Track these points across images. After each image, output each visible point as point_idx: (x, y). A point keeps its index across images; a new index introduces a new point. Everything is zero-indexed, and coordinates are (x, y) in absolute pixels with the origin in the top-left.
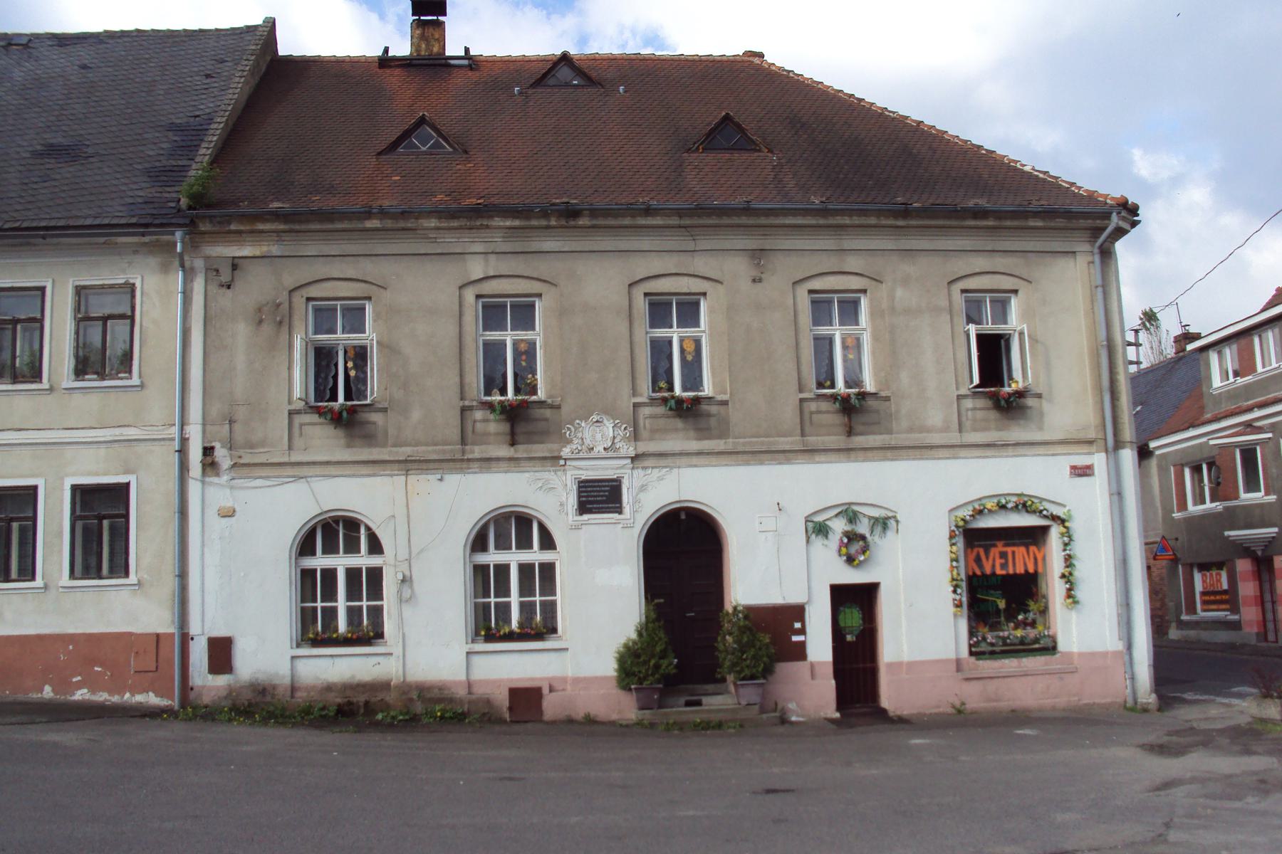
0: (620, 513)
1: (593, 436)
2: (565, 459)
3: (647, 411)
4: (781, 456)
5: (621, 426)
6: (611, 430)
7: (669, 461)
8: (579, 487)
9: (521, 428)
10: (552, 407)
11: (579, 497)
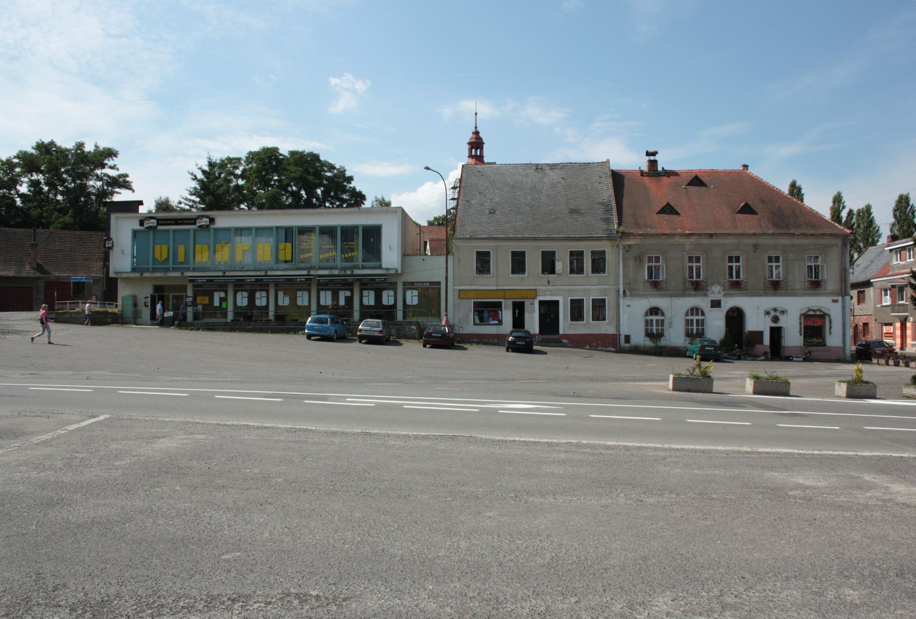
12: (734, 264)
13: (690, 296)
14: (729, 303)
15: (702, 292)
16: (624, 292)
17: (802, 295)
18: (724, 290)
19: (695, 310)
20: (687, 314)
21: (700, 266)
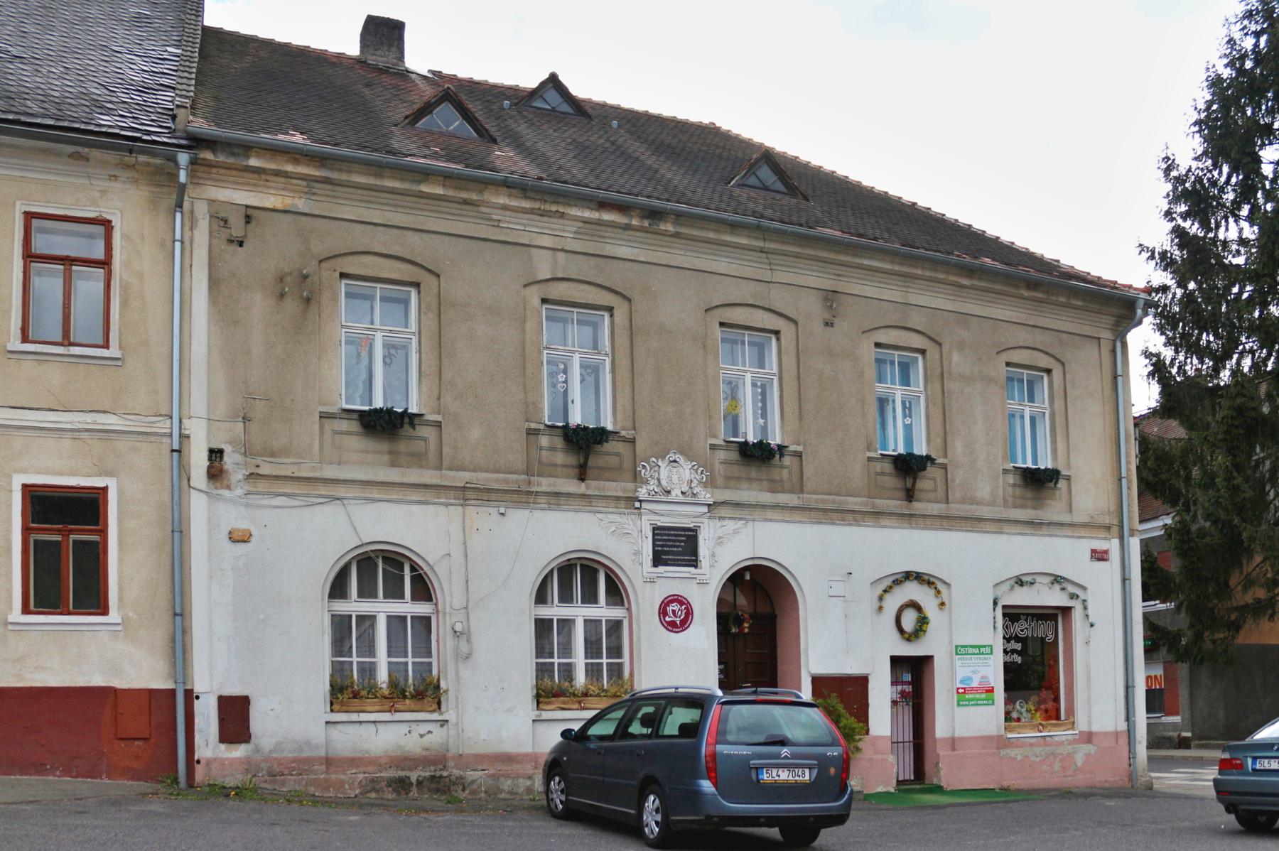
0: (696, 567)
1: (670, 478)
2: (640, 501)
3: (721, 455)
4: (850, 517)
5: (697, 469)
6: (687, 472)
7: (745, 513)
8: (654, 535)
10: (625, 440)
11: (654, 546)
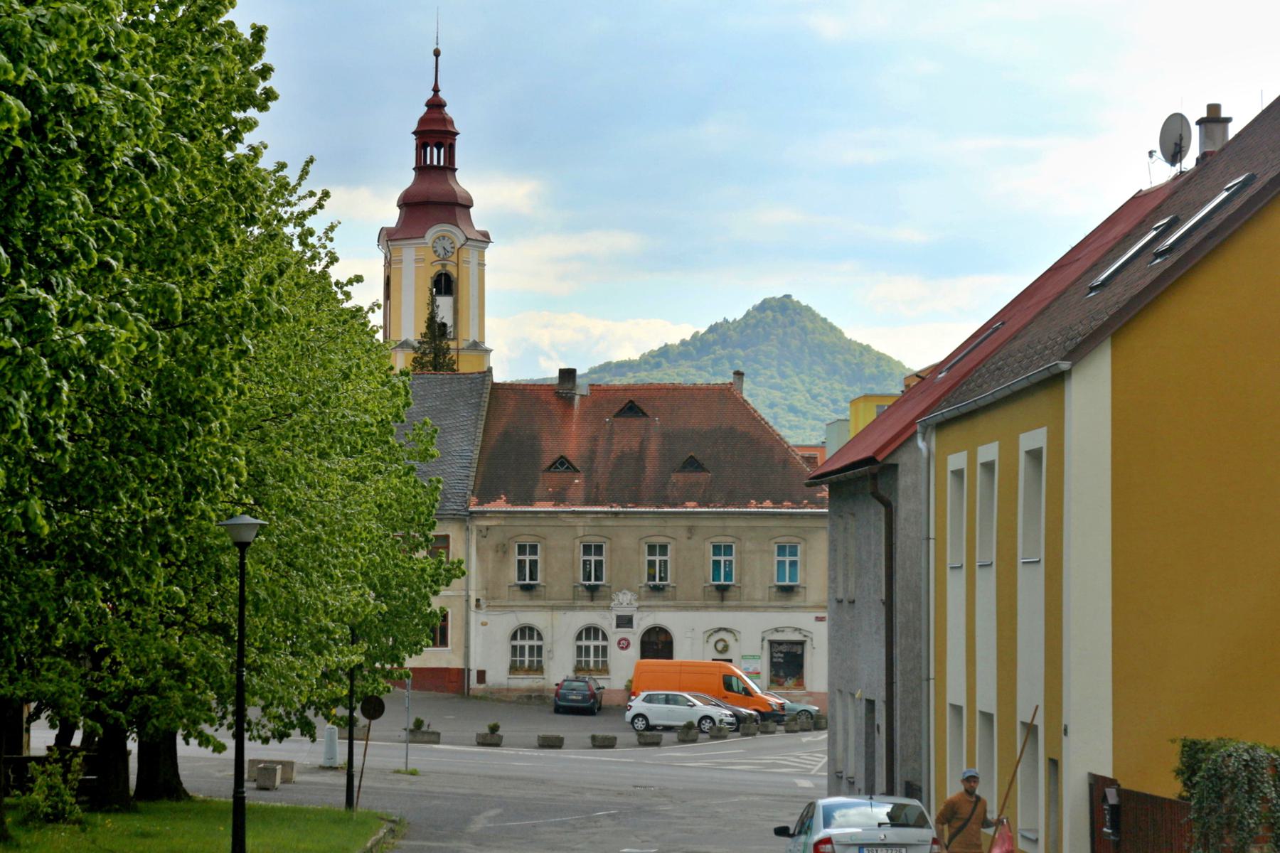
9: (595, 594)
12: (657, 558)
13: (583, 608)
14: (644, 621)
15: (603, 603)
16: (478, 600)
17: (766, 608)
18: (639, 599)
19: (591, 631)
20: (579, 637)
21: (601, 561)
